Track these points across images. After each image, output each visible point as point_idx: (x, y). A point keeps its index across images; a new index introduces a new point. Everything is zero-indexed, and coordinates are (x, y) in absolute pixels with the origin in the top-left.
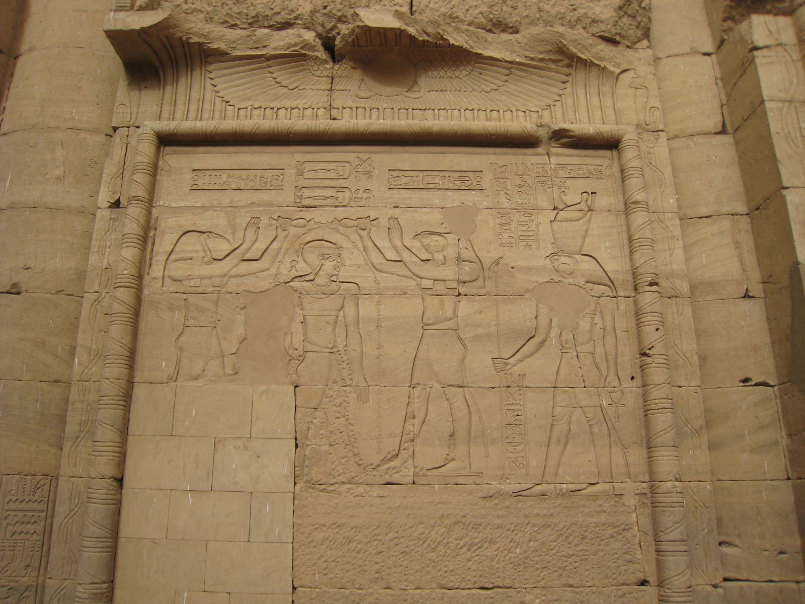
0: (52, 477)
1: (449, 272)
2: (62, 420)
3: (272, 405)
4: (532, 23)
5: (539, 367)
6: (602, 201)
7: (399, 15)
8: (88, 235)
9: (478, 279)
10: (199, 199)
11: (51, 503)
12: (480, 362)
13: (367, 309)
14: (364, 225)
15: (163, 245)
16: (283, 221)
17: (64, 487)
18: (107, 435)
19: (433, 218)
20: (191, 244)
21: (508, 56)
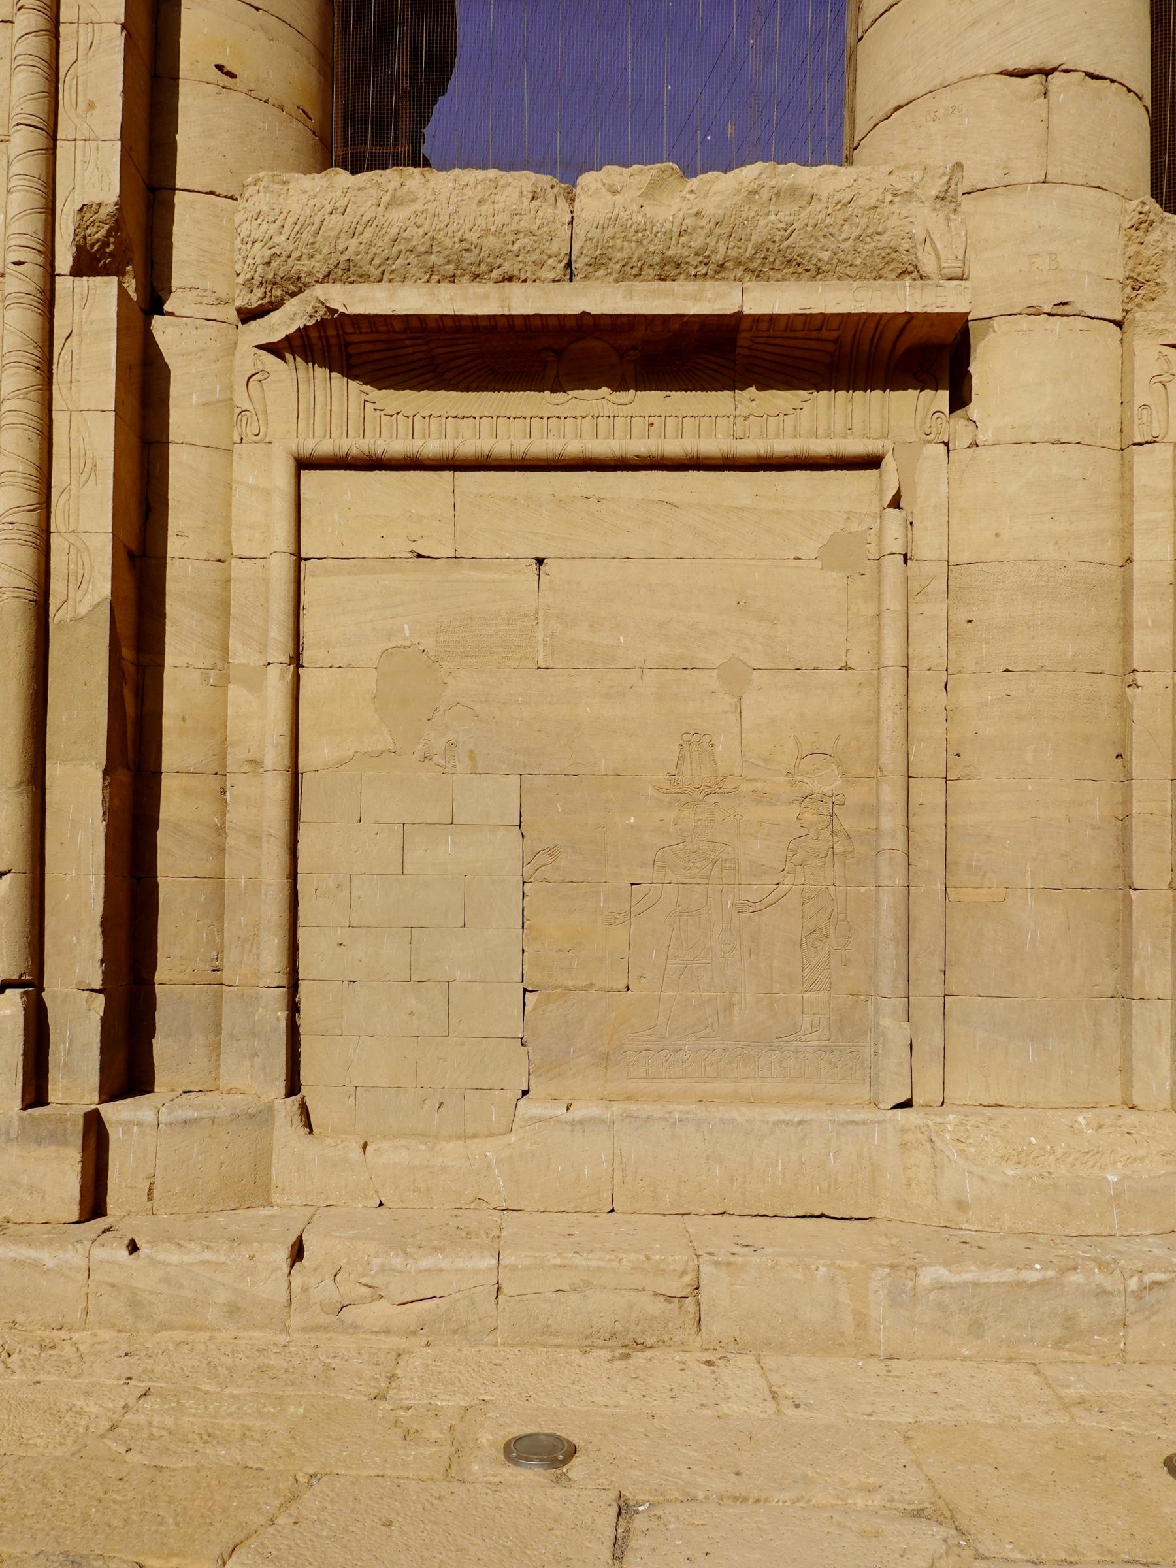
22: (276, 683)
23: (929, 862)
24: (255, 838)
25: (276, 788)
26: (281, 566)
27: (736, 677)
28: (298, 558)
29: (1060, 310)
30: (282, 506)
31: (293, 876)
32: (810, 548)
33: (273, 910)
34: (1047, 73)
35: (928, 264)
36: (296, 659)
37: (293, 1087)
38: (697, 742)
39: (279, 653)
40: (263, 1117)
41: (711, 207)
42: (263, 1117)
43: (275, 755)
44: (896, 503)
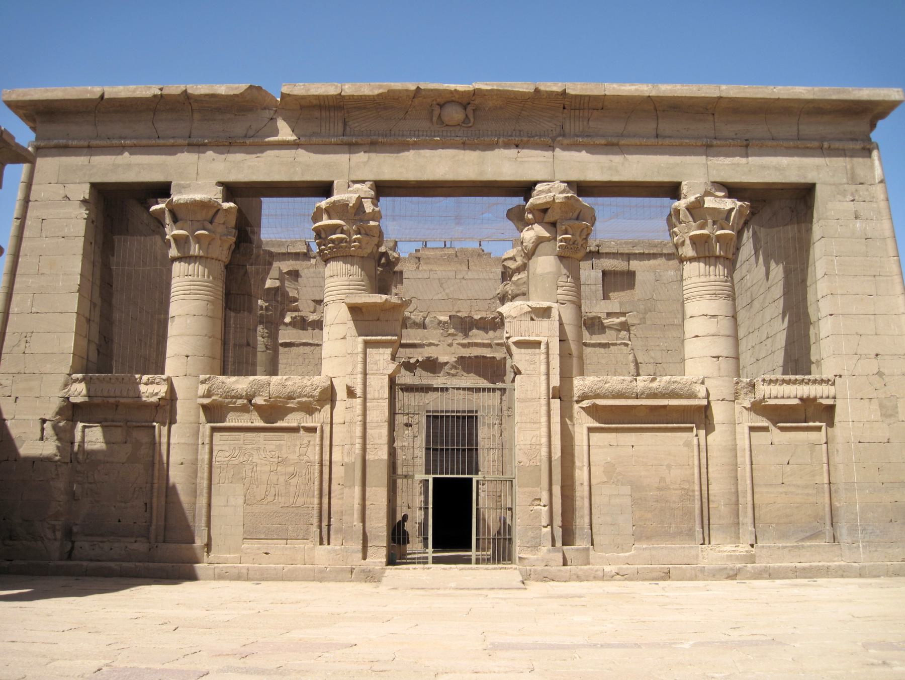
0: (195, 504)
1: (276, 460)
2: (196, 492)
3: (239, 488)
4: (299, 397)
5: (294, 481)
6: (312, 443)
7: (265, 400)
8: (197, 449)
9: (283, 462)
10: (222, 443)
11: (195, 509)
12: (282, 479)
13: (258, 468)
14: (258, 449)
15: (214, 454)
16: (240, 448)
17: (197, 505)
18: (205, 495)
19: (273, 447)
20: (220, 453)
21: (292, 405)
22: (586, 469)
23: (705, 500)
24: (582, 498)
25: (586, 488)
26: (585, 448)
27: (669, 467)
28: (589, 446)
29: (723, 400)
30: (585, 437)
31: (590, 505)
32: (681, 443)
33: (587, 512)
34: (718, 357)
35: (700, 395)
36: (589, 465)
37: (592, 544)
38: (662, 479)
39: (586, 464)
40: (588, 549)
41: (662, 385)
42: (588, 549)
43: (586, 483)
44: (697, 436)
